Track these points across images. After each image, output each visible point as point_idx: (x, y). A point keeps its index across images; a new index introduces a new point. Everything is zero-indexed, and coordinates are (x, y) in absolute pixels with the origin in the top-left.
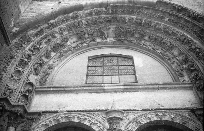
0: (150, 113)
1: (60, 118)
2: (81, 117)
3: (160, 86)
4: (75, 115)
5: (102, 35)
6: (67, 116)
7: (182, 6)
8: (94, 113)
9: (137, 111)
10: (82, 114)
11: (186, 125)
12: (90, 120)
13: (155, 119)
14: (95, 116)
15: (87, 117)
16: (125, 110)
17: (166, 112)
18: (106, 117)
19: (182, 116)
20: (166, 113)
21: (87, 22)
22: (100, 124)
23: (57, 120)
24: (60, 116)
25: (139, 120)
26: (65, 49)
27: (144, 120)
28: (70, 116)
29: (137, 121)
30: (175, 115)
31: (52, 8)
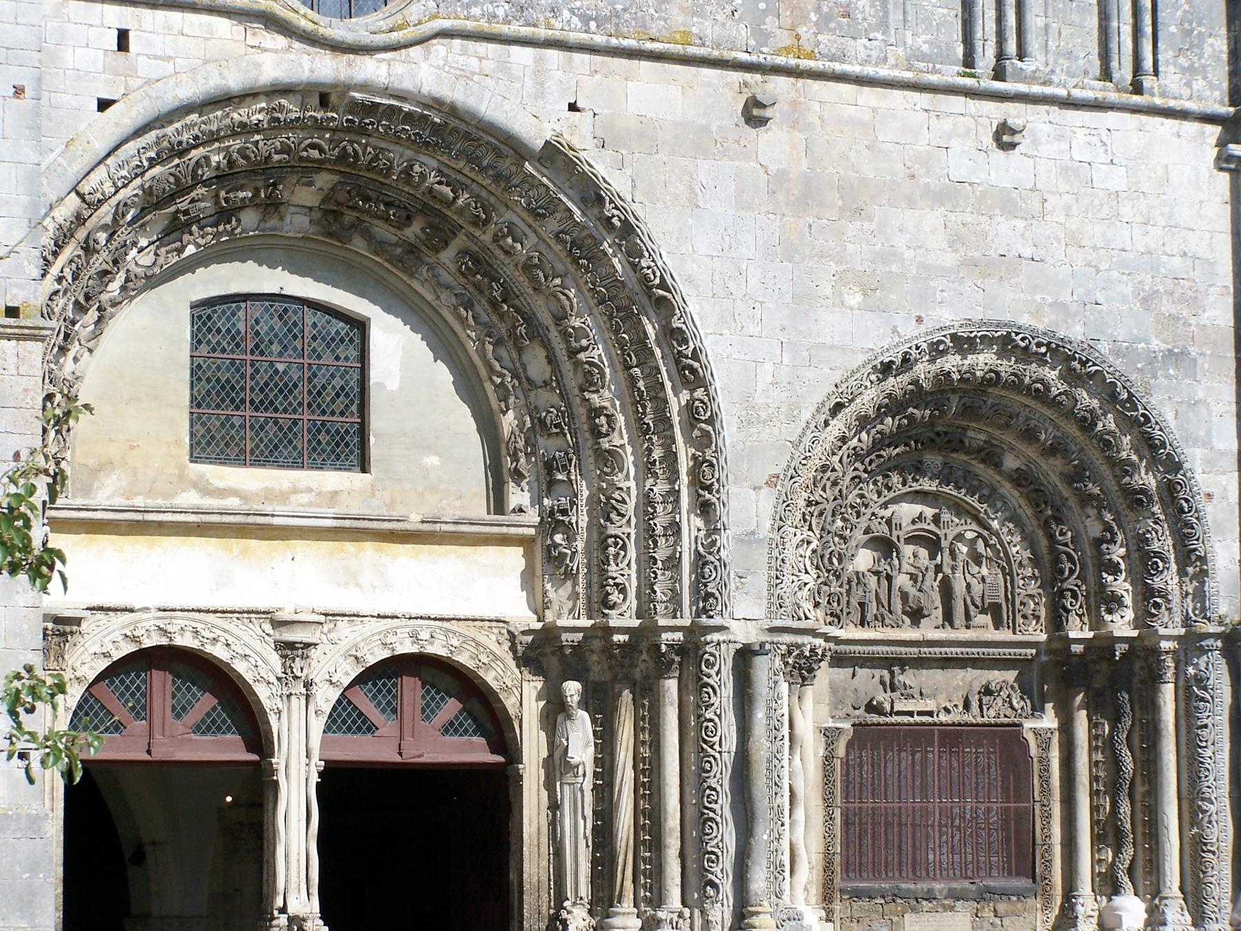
0: (397, 628)
1: (143, 632)
2: (203, 633)
3: (445, 527)
4: (187, 623)
5: (272, 206)
6: (162, 626)
7: (629, 199)
8: (238, 619)
9: (361, 619)
10: (206, 623)
11: (481, 673)
12: (228, 645)
13: (407, 647)
14: (240, 626)
15: (221, 633)
16: (326, 615)
17: (441, 628)
18: (271, 632)
19: (478, 644)
20: (438, 631)
21: (231, 163)
22: (258, 659)
23: (135, 639)
24: (143, 624)
25: (365, 651)
26: (114, 287)
27: (376, 651)
28: (169, 628)
29: (359, 654)
30: (461, 639)
31: (104, 105)
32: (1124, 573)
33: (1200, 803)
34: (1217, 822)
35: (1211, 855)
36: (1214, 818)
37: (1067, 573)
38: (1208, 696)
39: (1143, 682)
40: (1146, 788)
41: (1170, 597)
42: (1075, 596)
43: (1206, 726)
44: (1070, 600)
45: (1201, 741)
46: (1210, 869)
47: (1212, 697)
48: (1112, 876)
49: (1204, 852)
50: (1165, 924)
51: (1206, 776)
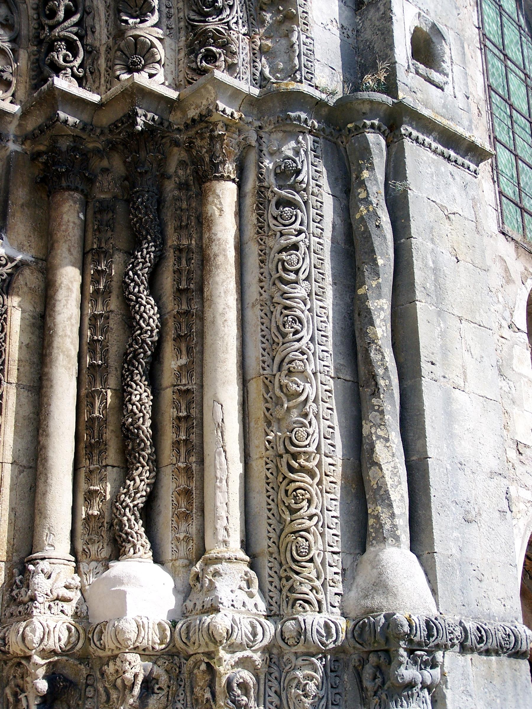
32: (156, 13)
33: (285, 381)
34: (316, 416)
35: (308, 479)
36: (311, 407)
37: (61, 14)
38: (298, 197)
39: (183, 186)
40: (183, 361)
41: (234, 48)
42: (72, 47)
43: (295, 247)
44: (64, 52)
45: (285, 270)
46: (305, 503)
47: (305, 203)
48: (111, 525)
49: (291, 469)
50: (218, 611)
51: (296, 332)
